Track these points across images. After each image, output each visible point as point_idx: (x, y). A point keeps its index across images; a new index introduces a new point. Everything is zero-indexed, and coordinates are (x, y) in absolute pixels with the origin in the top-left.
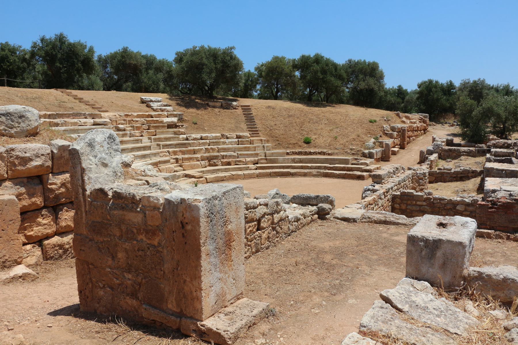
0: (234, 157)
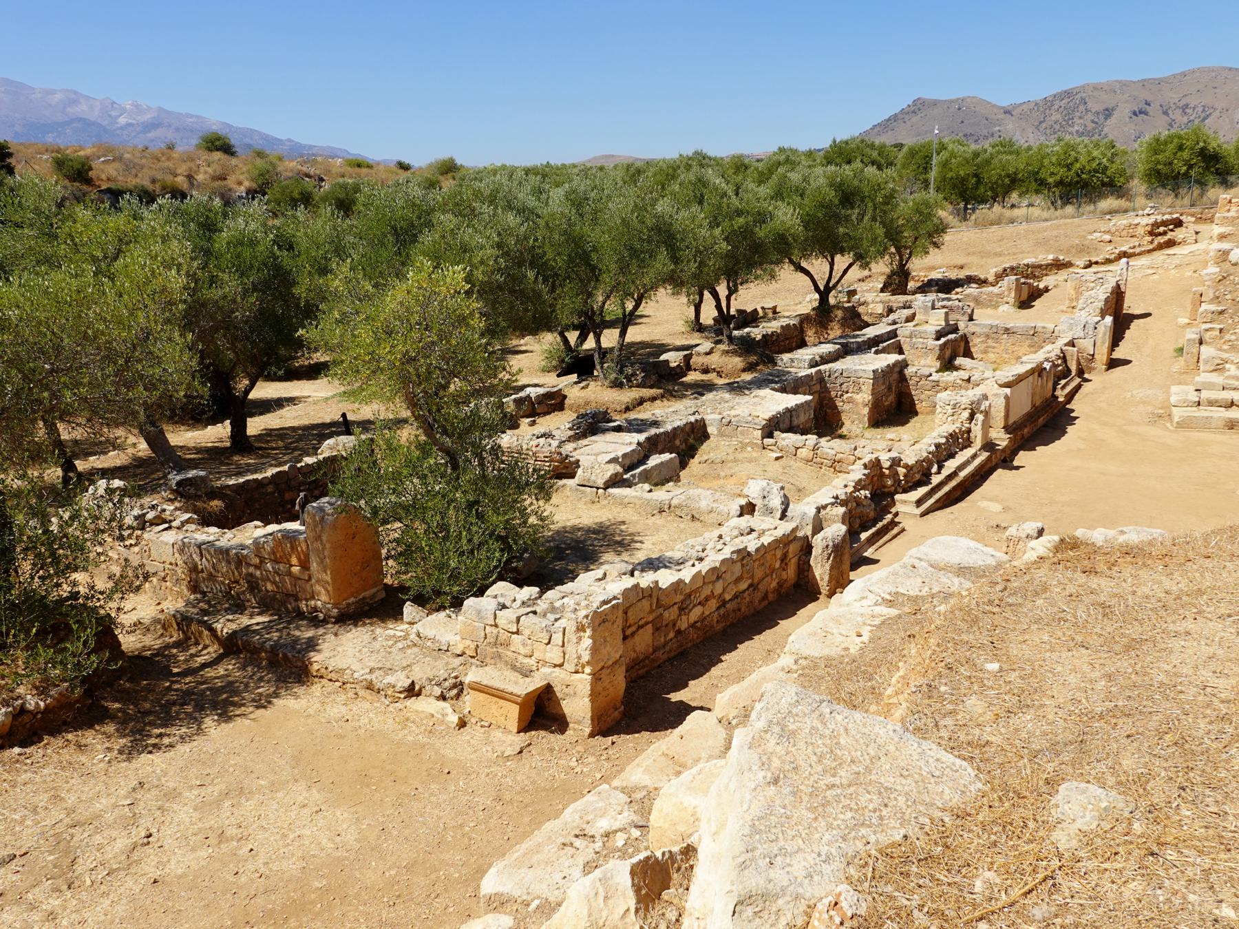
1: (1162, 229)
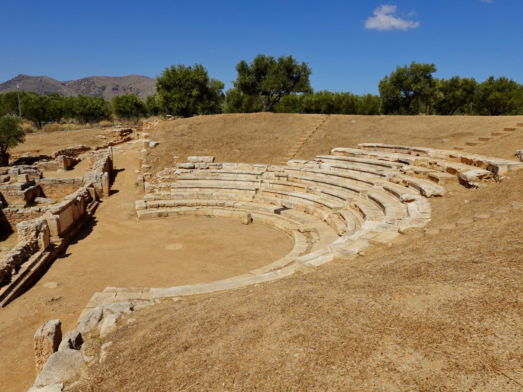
1: (125, 133)
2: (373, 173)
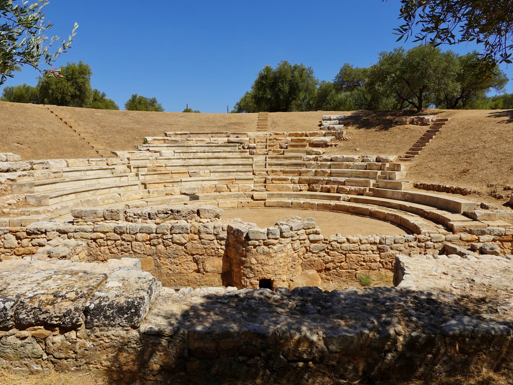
0: (340, 183)
2: (229, 152)
